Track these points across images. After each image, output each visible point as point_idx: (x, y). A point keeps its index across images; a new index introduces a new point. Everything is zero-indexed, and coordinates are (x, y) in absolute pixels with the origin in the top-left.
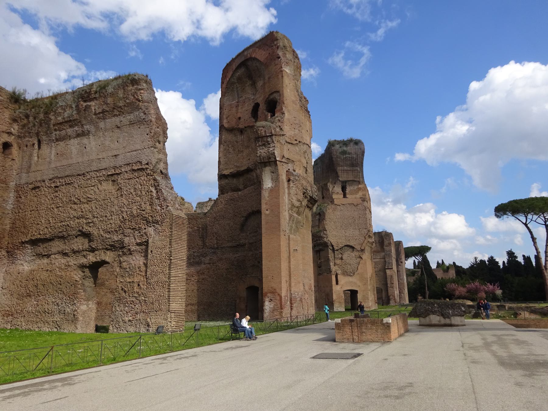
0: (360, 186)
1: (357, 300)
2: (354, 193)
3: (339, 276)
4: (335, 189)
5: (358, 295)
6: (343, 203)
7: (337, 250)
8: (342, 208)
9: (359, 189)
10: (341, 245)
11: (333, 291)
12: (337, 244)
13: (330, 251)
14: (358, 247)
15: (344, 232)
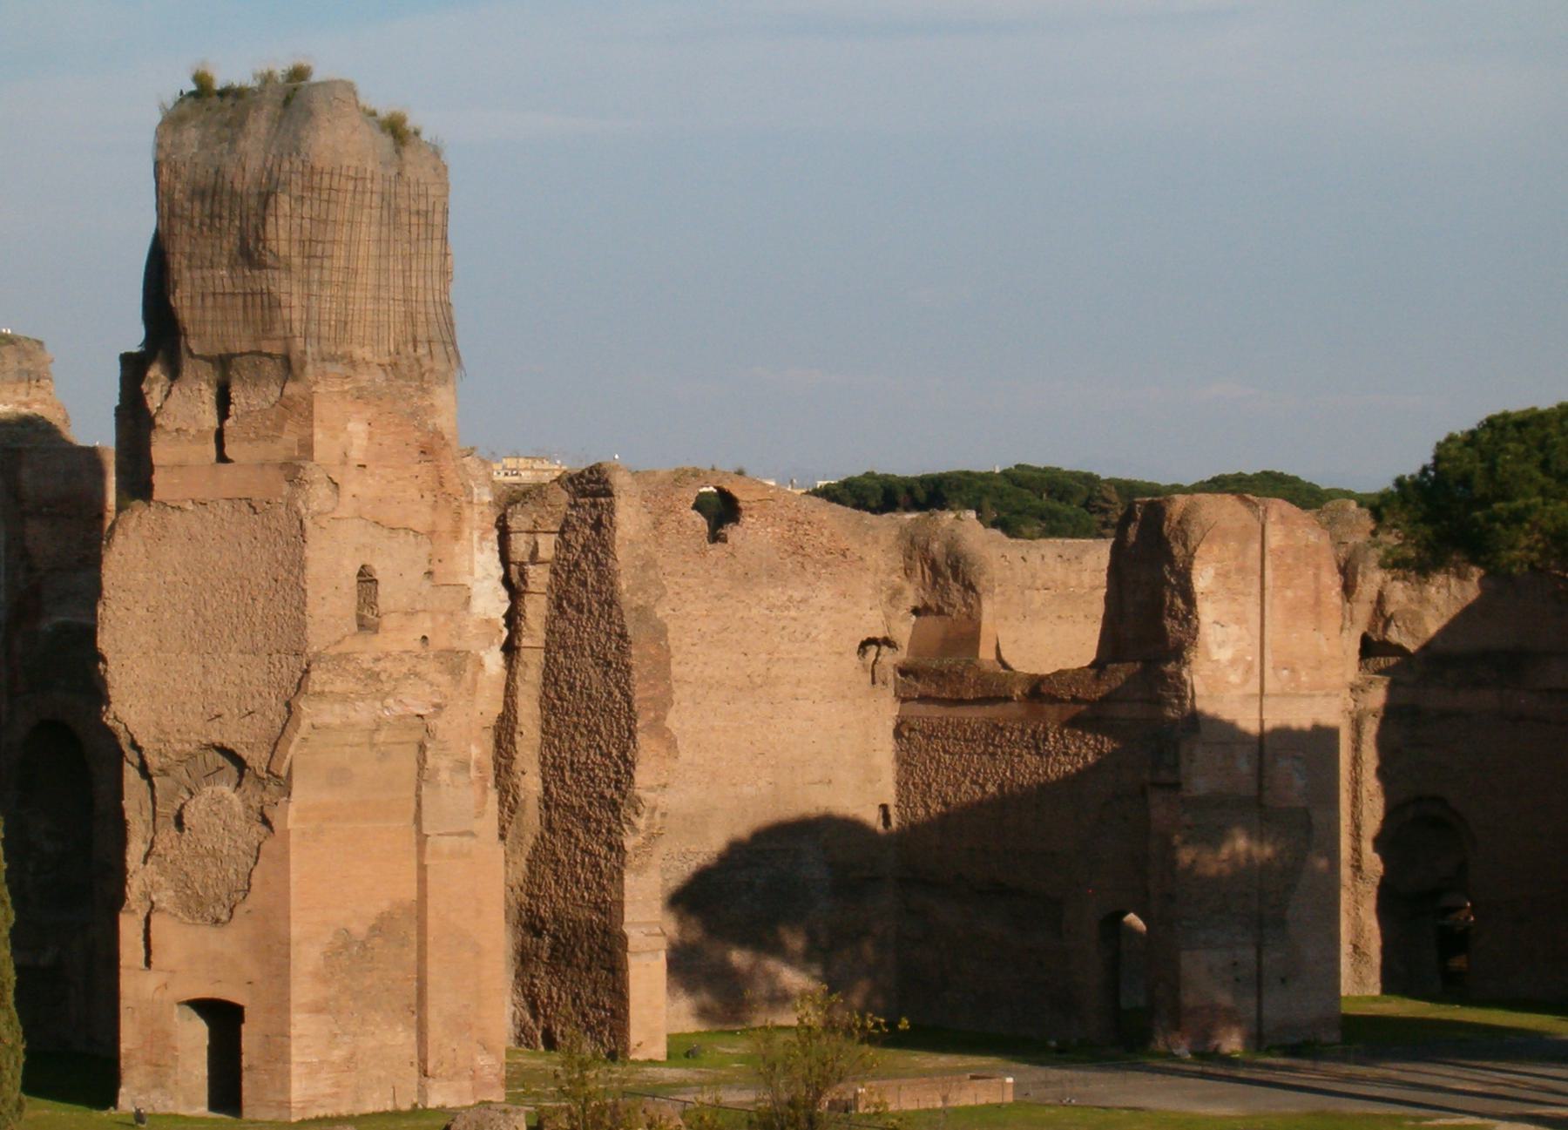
0: (292, 389)
1: (240, 1060)
2: (263, 432)
3: (156, 920)
4: (172, 404)
5: (244, 1028)
6: (199, 497)
7: (164, 772)
8: (196, 527)
9: (286, 405)
10: (178, 747)
11: (124, 1004)
12: (159, 740)
13: (131, 775)
14: (256, 759)
15: (198, 669)
